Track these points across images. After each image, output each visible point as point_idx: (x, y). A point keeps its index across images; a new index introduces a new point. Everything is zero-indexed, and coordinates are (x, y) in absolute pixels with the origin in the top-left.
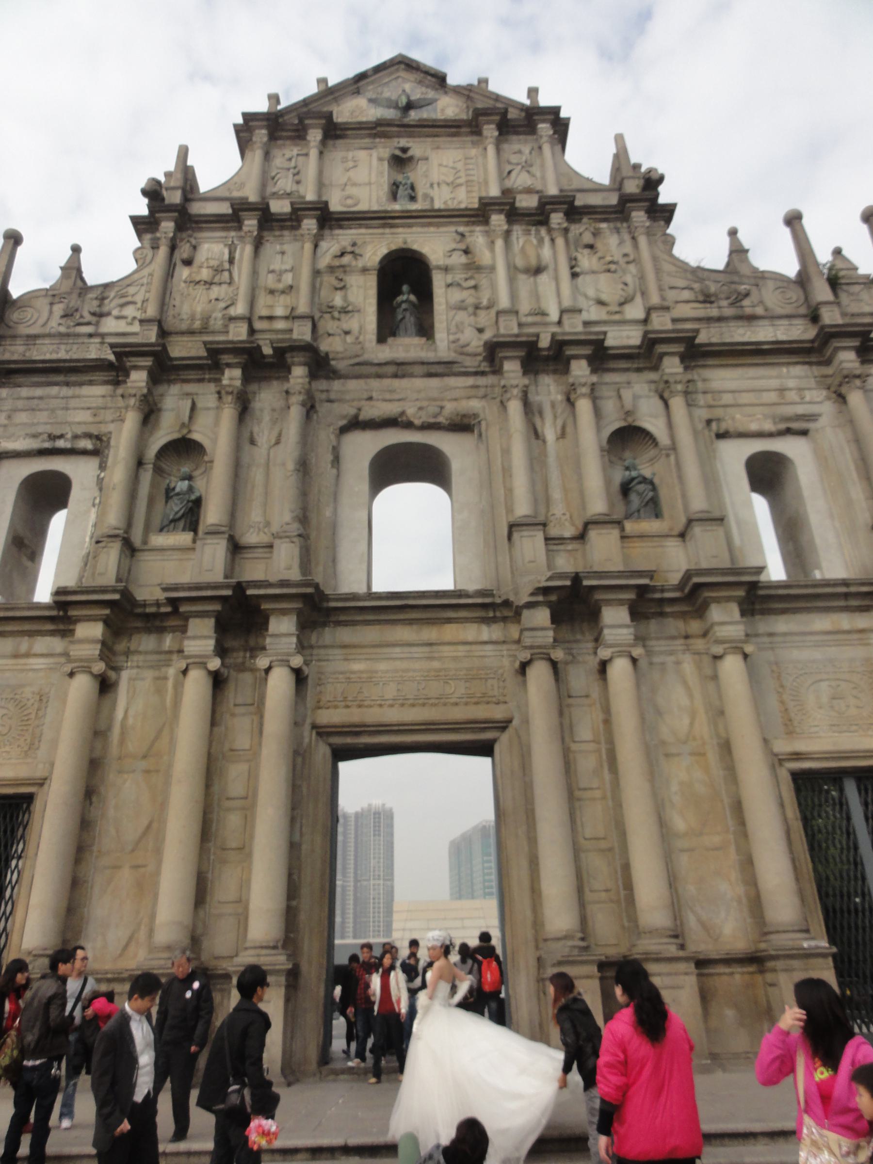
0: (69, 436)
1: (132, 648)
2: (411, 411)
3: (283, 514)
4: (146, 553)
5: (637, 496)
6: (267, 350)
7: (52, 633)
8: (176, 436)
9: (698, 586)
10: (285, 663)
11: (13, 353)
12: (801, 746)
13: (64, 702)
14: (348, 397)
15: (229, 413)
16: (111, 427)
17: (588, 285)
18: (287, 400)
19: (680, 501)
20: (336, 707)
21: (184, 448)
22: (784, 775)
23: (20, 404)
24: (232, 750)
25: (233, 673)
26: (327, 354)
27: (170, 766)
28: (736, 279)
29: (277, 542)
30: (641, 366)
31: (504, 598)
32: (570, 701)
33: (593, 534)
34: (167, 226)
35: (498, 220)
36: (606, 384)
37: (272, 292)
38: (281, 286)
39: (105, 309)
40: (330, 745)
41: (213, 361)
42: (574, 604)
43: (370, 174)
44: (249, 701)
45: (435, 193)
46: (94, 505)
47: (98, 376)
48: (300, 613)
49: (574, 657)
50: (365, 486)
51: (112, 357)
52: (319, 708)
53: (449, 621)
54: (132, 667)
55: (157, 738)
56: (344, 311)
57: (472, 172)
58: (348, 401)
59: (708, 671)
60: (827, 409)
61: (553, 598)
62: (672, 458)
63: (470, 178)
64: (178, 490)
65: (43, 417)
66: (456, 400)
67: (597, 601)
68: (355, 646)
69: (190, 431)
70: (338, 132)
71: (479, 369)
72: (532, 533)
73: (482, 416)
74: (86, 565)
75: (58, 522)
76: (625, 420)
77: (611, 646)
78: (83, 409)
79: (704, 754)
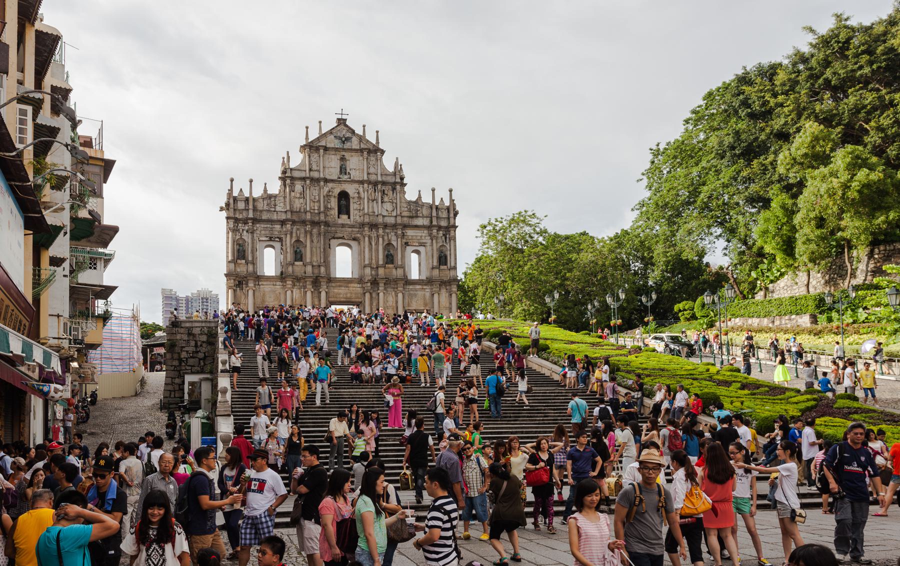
5: (390, 259)
17: (385, 205)
21: (298, 241)
34: (288, 181)
35: (366, 185)
41: (304, 222)
42: (375, 282)
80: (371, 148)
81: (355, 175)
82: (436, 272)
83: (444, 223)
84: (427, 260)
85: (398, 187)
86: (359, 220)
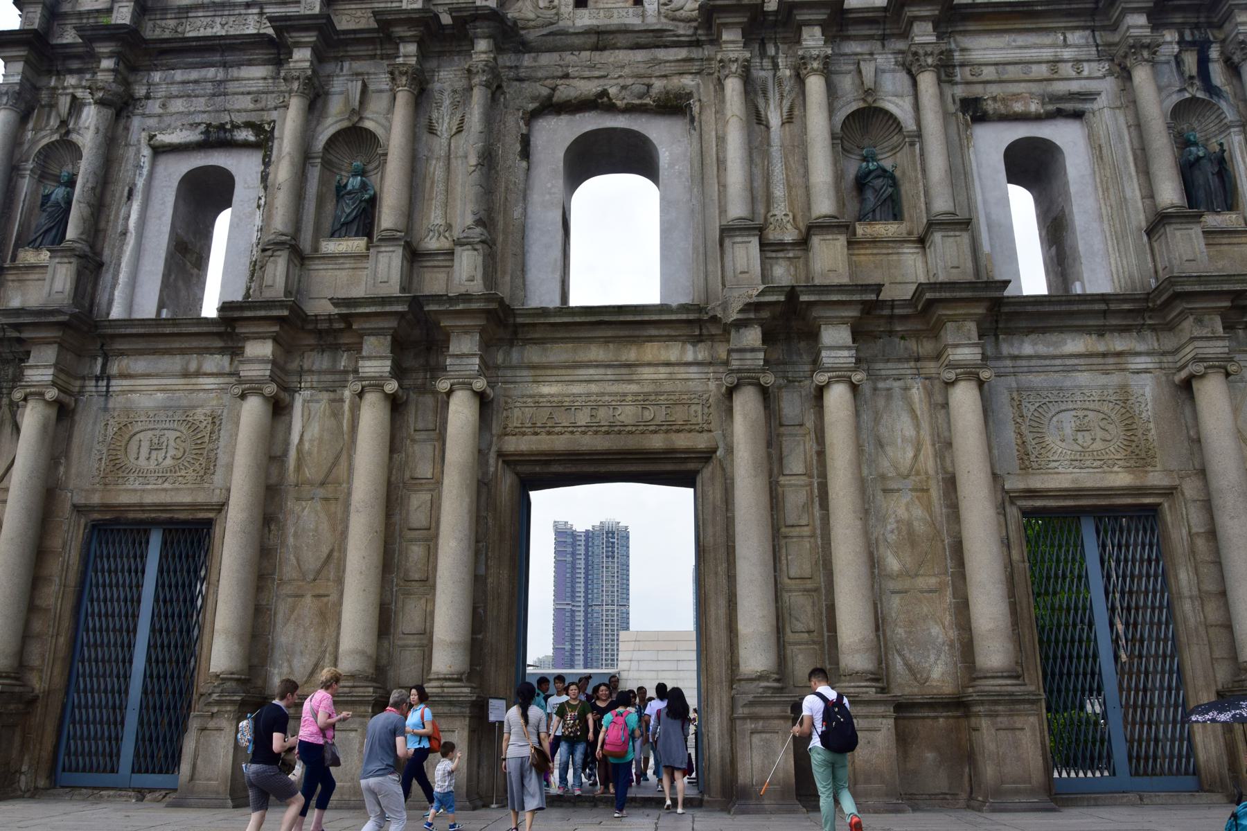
0: (228, 126)
1: (306, 367)
2: (612, 91)
3: (464, 215)
4: (317, 262)
5: (874, 194)
6: (446, 19)
7: (222, 351)
8: (345, 124)
9: (931, 303)
10: (467, 386)
11: (163, 29)
12: (1037, 483)
13: (237, 424)
14: (540, 75)
15: (403, 98)
16: (274, 115)
18: (470, 79)
19: (922, 199)
20: (524, 434)
22: (1013, 512)
23: (174, 89)
24: (413, 479)
25: (413, 396)
26: (515, 23)
27: (349, 494)
29: (458, 250)
30: (888, 32)
31: (711, 314)
32: (782, 429)
33: (816, 240)
36: (846, 55)
40: (517, 474)
41: (383, 35)
42: (788, 321)
44: (431, 426)
46: (259, 207)
47: (259, 54)
48: (483, 331)
49: (789, 381)
50: (560, 183)
51: (270, 31)
52: (506, 435)
53: (651, 339)
54: (307, 388)
55: (335, 463)
58: (540, 79)
59: (939, 398)
60: (1108, 87)
62: (917, 146)
64: (349, 187)
65: (200, 104)
66: (665, 76)
67: (815, 318)
68: (544, 367)
69: (361, 119)
71: (694, 38)
72: (746, 239)
73: (696, 96)
74: (252, 275)
75: (223, 221)
76: (864, 100)
77: (828, 370)
78: (243, 93)
79: (928, 490)
84: (1108, 182)
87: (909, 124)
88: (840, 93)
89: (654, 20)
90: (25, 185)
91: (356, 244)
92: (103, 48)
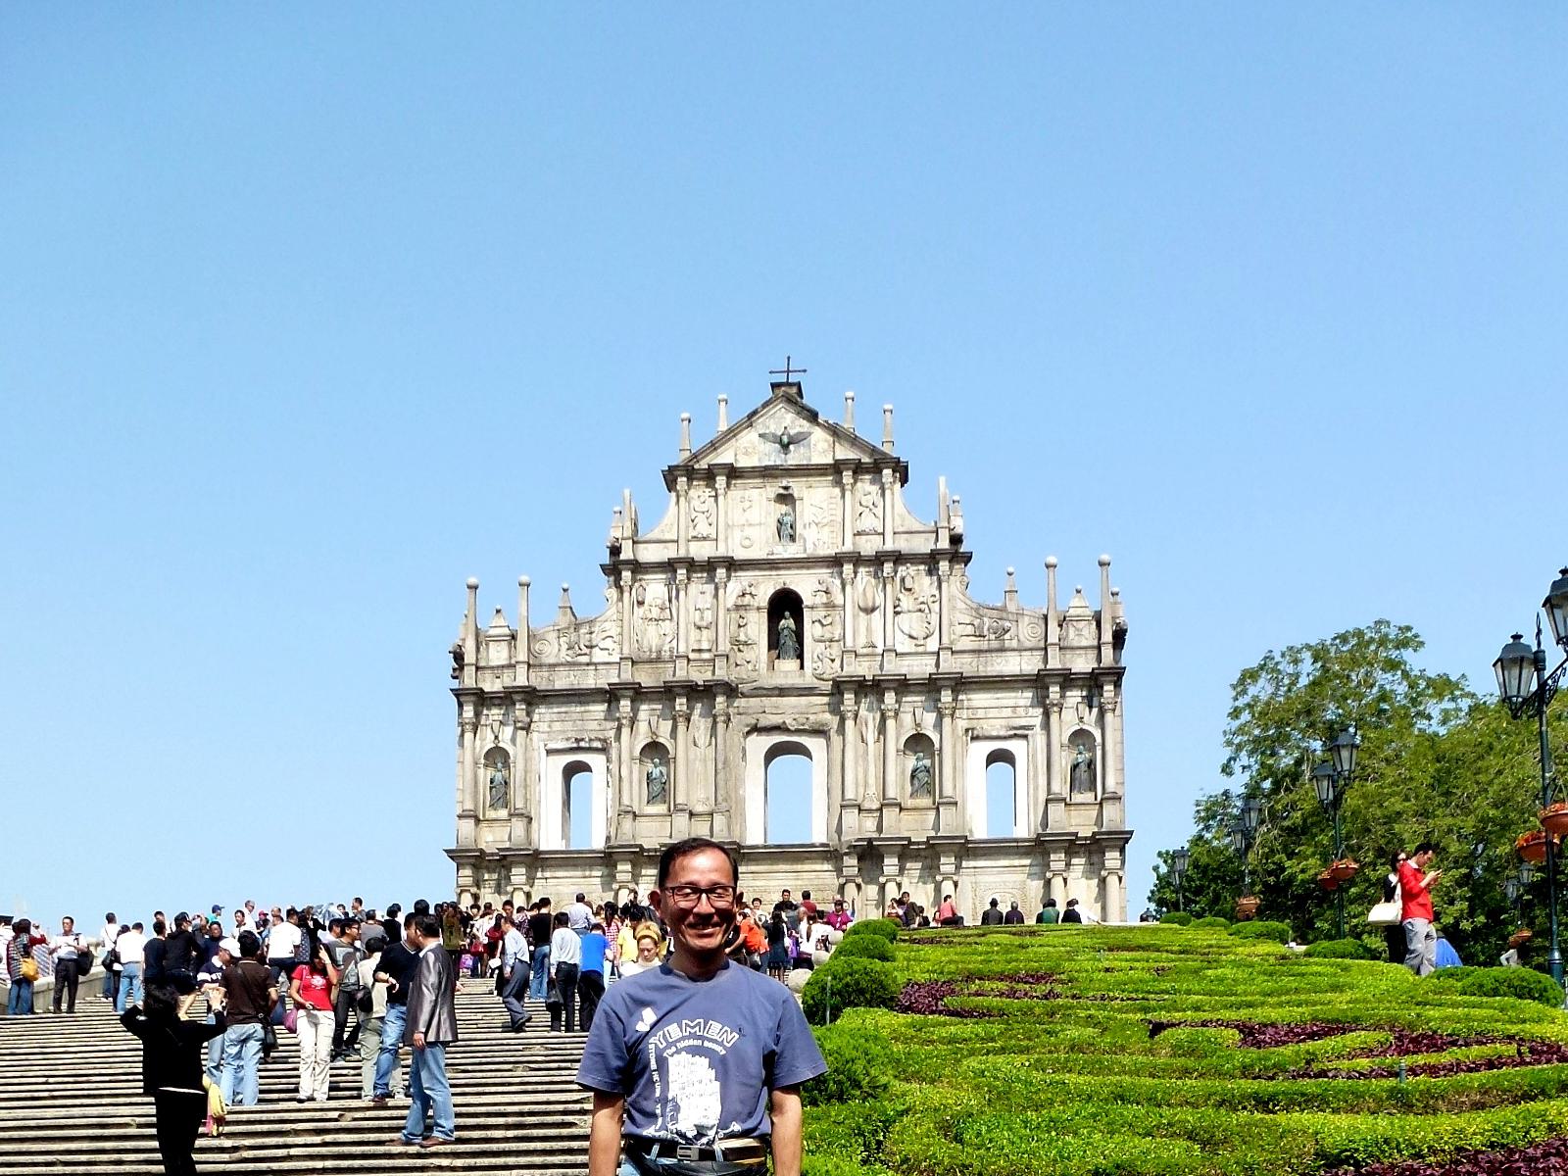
0: (587, 739)
2: (787, 722)
8: (650, 740)
14: (750, 712)
21: (654, 749)
28: (1004, 615)
35: (848, 568)
37: (699, 628)
38: (704, 624)
39: (594, 643)
41: (667, 693)
43: (761, 515)
45: (806, 533)
53: (808, 859)
56: (746, 644)
57: (834, 512)
61: (859, 850)
63: (833, 518)
65: (569, 725)
70: (737, 474)
80: (866, 459)
81: (819, 540)
82: (1057, 811)
83: (1083, 664)
84: (1032, 778)
85: (944, 566)
86: (832, 670)
87: (937, 746)
88: (905, 724)
89: (810, 681)
90: (481, 771)
91: (661, 808)
92: (516, 697)
